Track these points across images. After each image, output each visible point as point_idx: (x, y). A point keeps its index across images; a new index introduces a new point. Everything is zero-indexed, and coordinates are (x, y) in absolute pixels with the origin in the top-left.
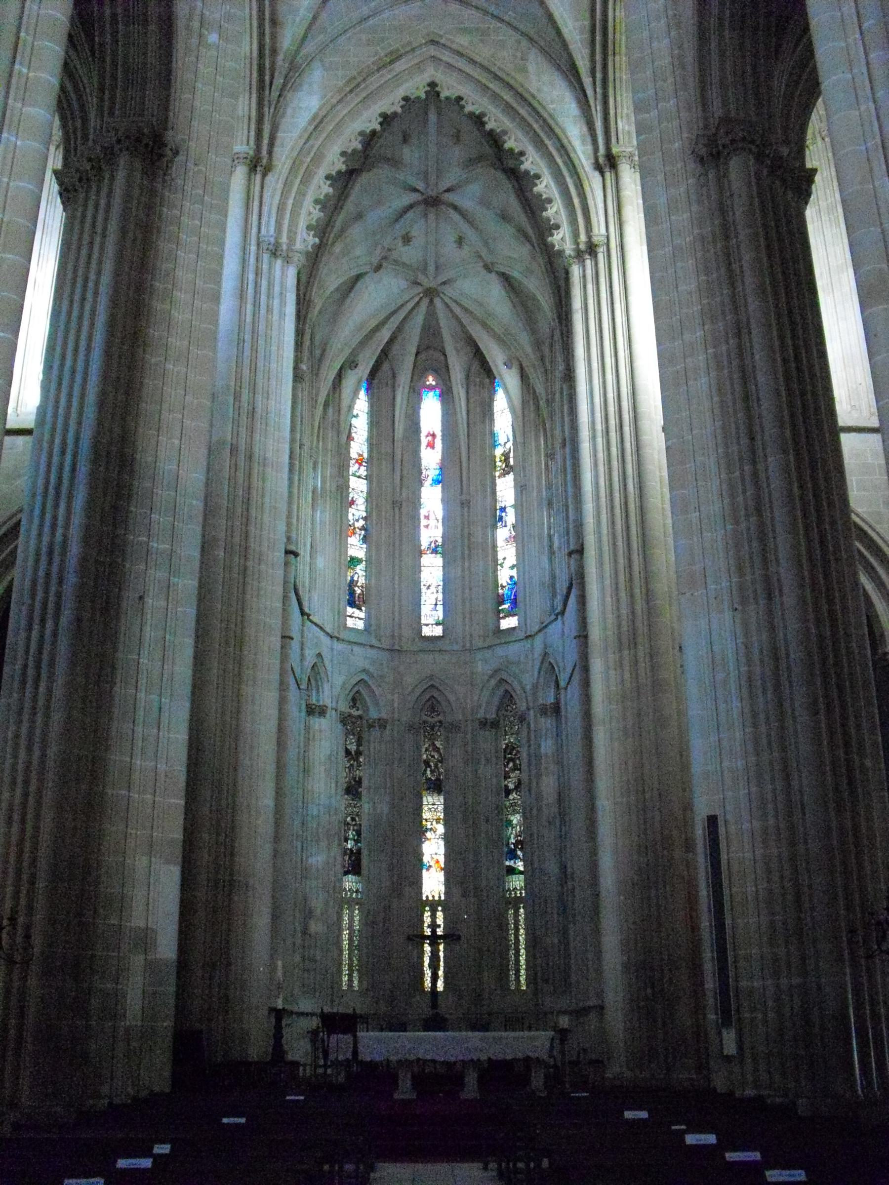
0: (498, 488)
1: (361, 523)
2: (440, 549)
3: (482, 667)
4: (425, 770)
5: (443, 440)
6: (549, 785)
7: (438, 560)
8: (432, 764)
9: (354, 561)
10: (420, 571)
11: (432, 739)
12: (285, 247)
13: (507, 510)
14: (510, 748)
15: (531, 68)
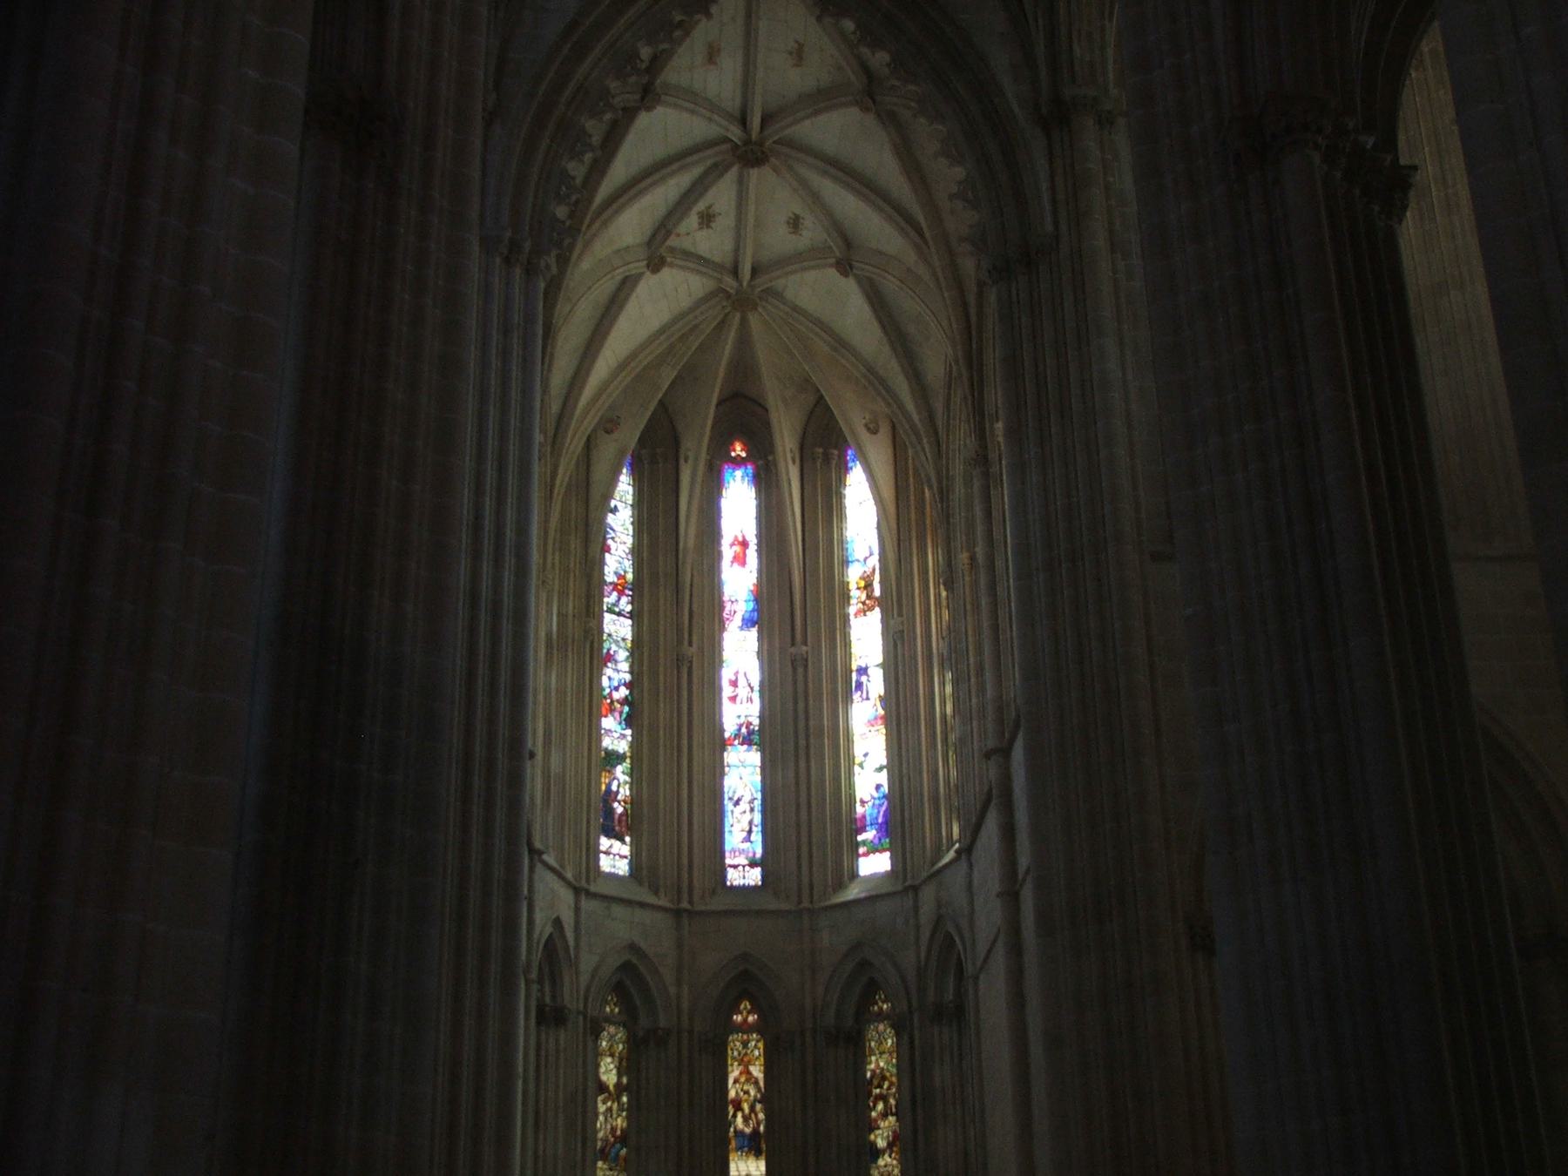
2: (756, 738)
4: (735, 1116)
5: (759, 551)
7: (754, 757)
8: (746, 1107)
9: (613, 758)
10: (722, 774)
11: (745, 1063)
12: (527, 245)
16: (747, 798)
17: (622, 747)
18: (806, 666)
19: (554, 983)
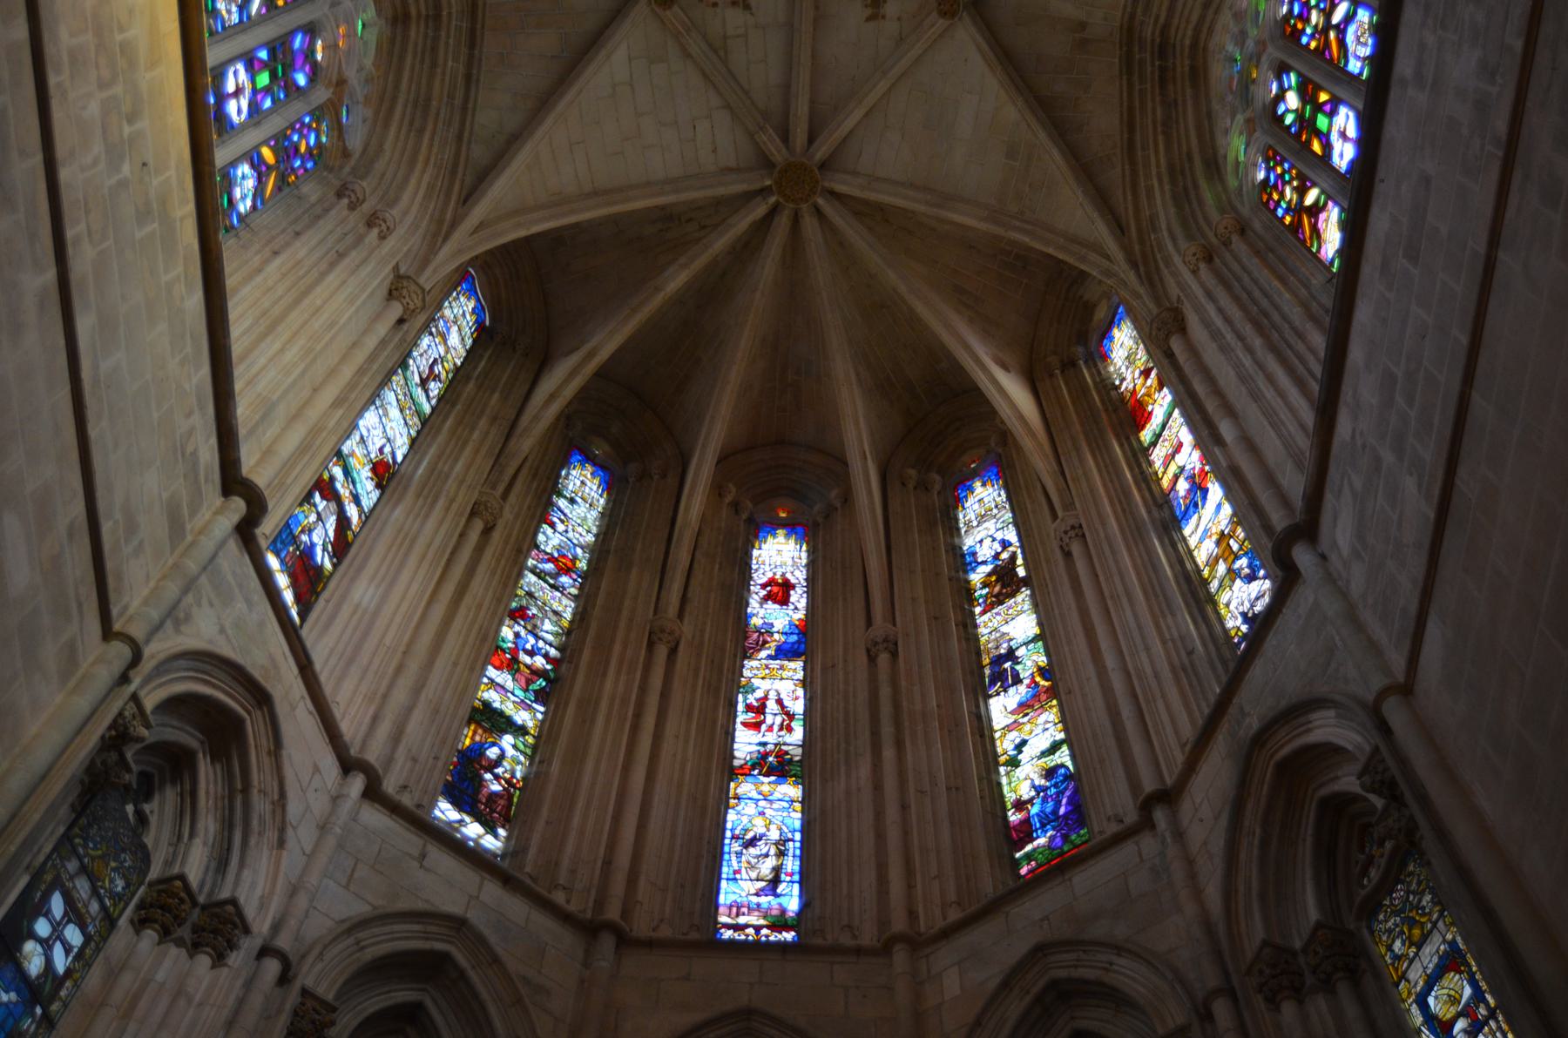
0: (982, 630)
1: (539, 661)
2: (796, 769)
9: (496, 722)
13: (1018, 653)
16: (774, 835)
17: (522, 717)
18: (894, 654)
19: (220, 863)
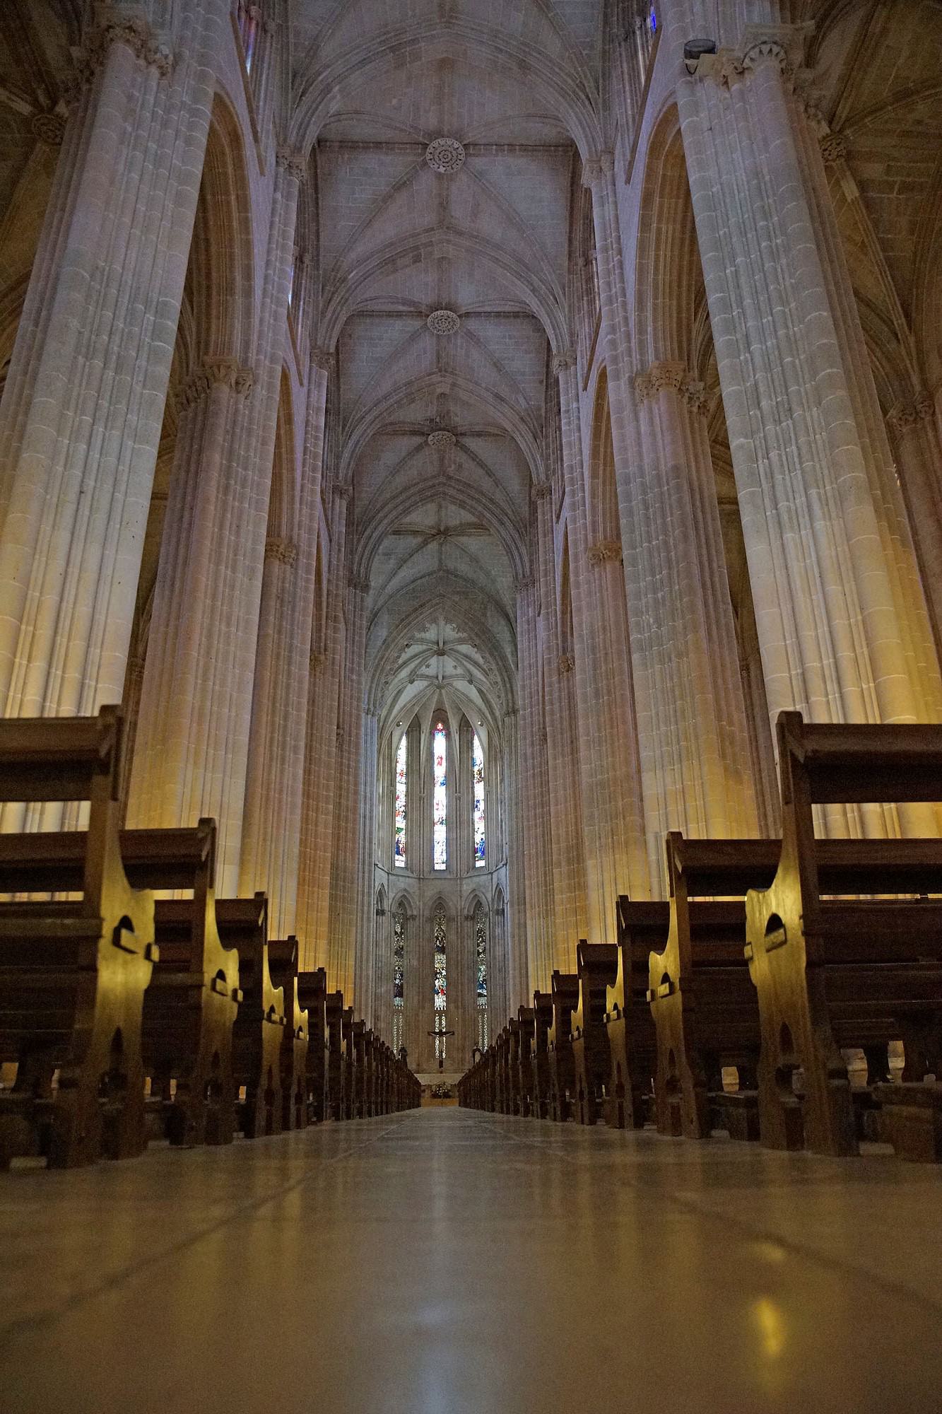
3: (467, 887)
6: (499, 951)
7: (443, 828)
9: (400, 830)
11: (440, 925)
14: (480, 931)
15: (489, 614)
